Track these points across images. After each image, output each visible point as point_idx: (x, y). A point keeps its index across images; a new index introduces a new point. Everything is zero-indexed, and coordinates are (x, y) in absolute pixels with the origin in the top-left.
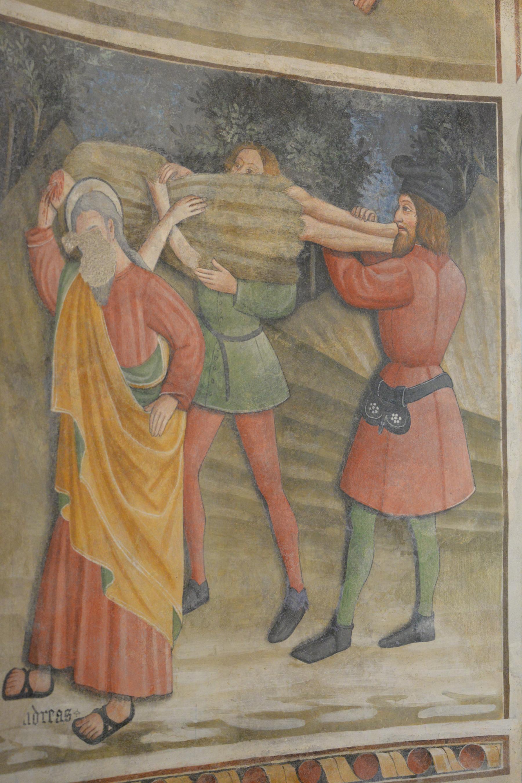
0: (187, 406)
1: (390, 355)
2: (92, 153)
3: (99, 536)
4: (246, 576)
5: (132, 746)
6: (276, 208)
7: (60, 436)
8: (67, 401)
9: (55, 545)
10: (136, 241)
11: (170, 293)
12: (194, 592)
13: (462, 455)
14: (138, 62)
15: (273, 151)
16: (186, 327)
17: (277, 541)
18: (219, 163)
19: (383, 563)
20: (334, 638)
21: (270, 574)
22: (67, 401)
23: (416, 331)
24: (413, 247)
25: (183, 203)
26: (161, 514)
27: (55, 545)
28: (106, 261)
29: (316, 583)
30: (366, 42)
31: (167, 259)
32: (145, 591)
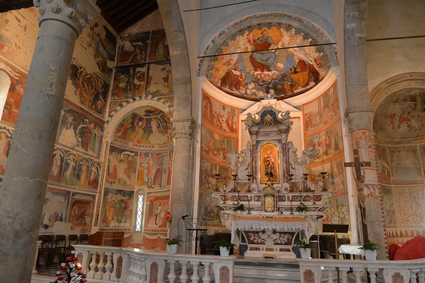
0: (113, 208)
1: (126, 206)
2: (110, 194)
3: (107, 215)
4: (116, 218)
5: (108, 227)
6: (120, 197)
7: (106, 210)
8: (107, 208)
9: (105, 215)
10: (111, 199)
11: (113, 202)
12: (113, 218)
13: (130, 212)
14: (113, 189)
15: (120, 194)
16: (114, 204)
17: (118, 216)
18: (117, 195)
19: (124, 218)
20: (121, 222)
21: (117, 218)
22: (107, 208)
23: (128, 204)
24: (129, 199)
25: (114, 196)
26: (111, 214)
27: (105, 215)
28: (110, 200)
29: (120, 218)
30: (127, 187)
31: (113, 200)
32: (110, 218)
